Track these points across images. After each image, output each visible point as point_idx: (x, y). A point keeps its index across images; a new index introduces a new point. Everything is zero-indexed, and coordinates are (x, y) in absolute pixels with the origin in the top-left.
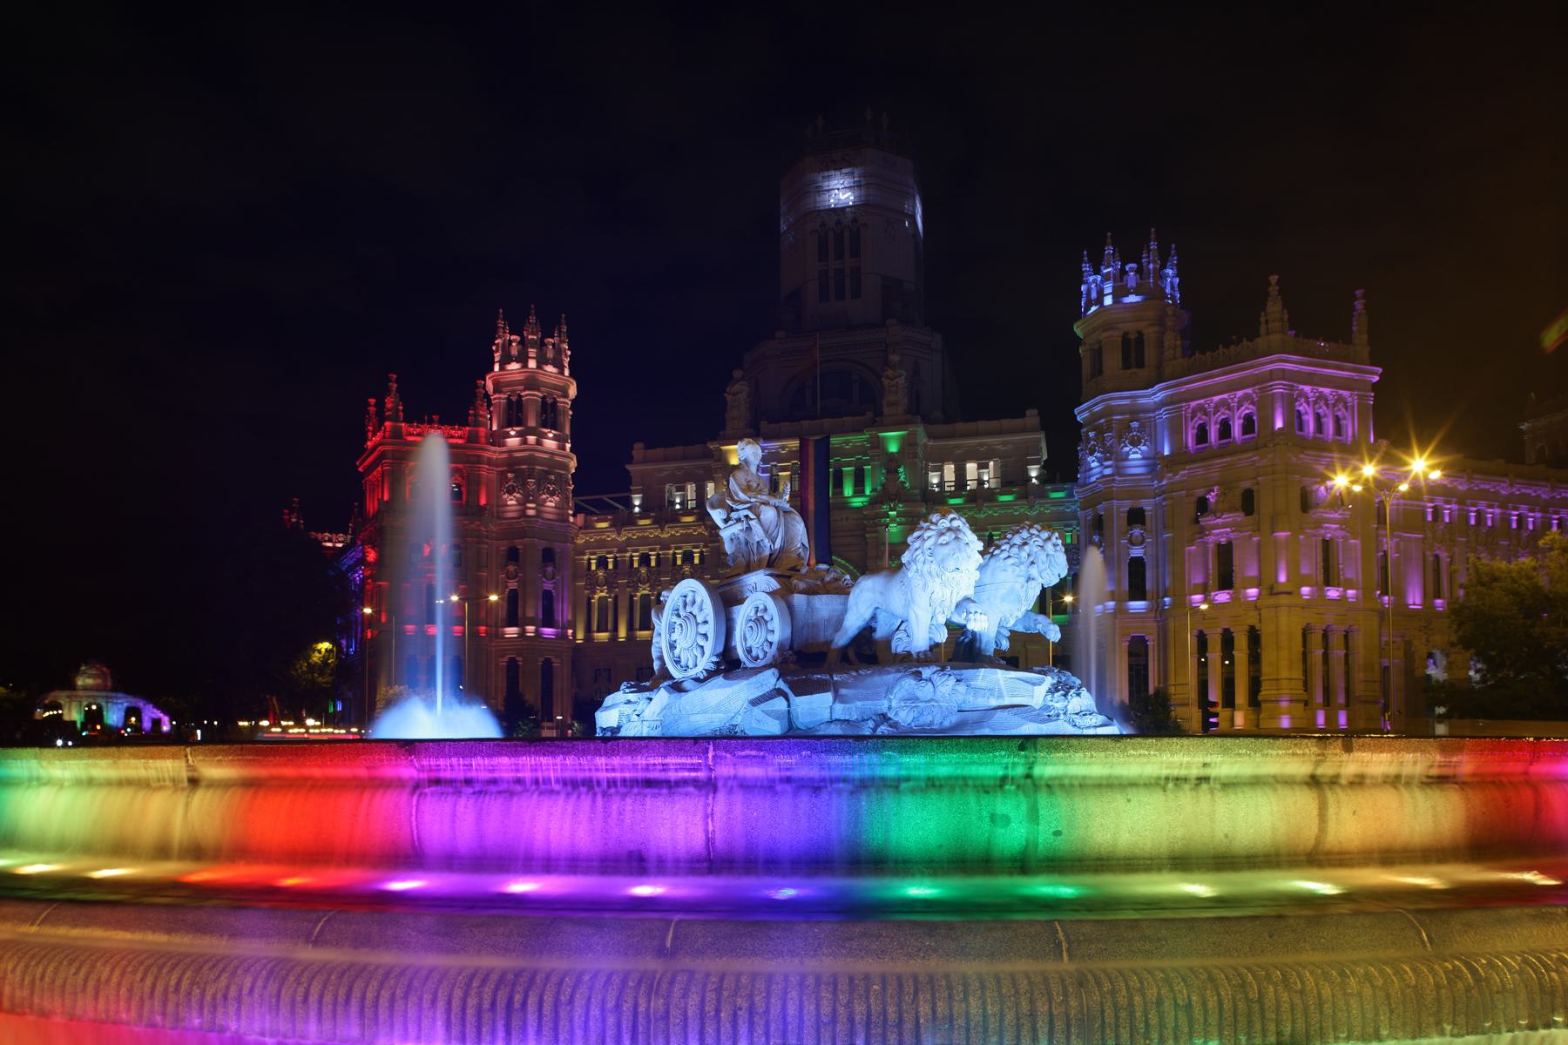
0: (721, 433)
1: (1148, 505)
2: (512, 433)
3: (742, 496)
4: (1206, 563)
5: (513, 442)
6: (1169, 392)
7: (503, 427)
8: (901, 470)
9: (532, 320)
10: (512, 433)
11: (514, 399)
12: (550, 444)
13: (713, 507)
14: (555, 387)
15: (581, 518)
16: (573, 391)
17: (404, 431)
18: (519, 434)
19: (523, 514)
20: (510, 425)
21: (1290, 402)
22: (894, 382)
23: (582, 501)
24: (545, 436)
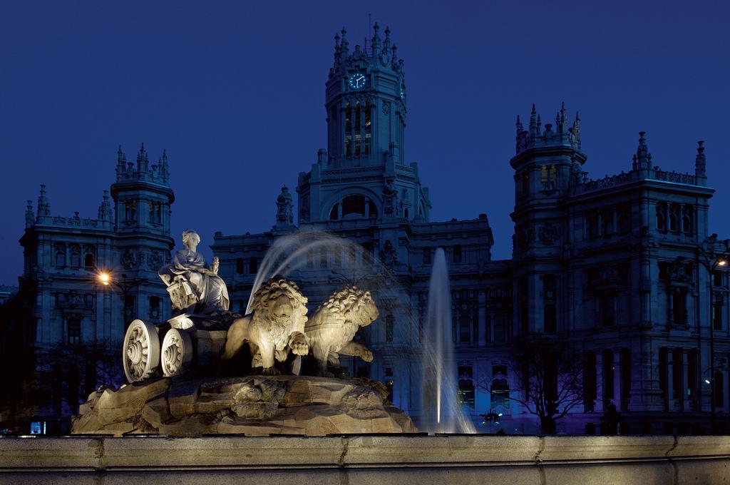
3: (181, 267)
13: (162, 274)
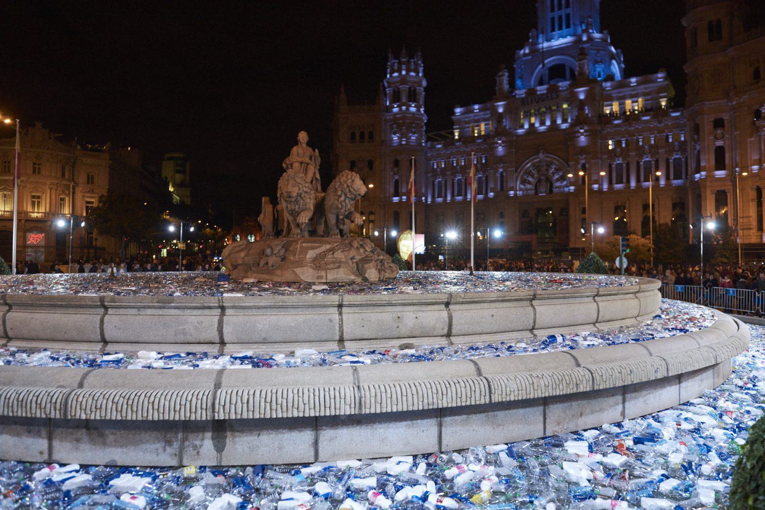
0: (494, 97)
1: (726, 117)
2: (395, 106)
4: (760, 147)
5: (396, 110)
9: (404, 51)
10: (395, 106)
11: (396, 90)
12: (413, 109)
14: (415, 82)
15: (429, 144)
19: (401, 144)
20: (395, 102)
23: (434, 135)
24: (408, 106)
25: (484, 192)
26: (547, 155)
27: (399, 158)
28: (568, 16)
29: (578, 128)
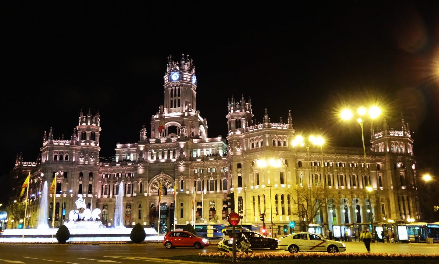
1: (242, 163)
2: (83, 142)
5: (83, 144)
6: (245, 135)
7: (80, 140)
8: (184, 152)
10: (83, 142)
12: (93, 144)
14: (95, 129)
15: (101, 164)
16: (100, 129)
17: (53, 142)
18: (84, 142)
19: (84, 164)
20: (82, 140)
21: (270, 139)
22: (183, 129)
24: (91, 142)
25: (131, 193)
26: (165, 175)
27: (83, 172)
28: (179, 101)
29: (180, 162)
